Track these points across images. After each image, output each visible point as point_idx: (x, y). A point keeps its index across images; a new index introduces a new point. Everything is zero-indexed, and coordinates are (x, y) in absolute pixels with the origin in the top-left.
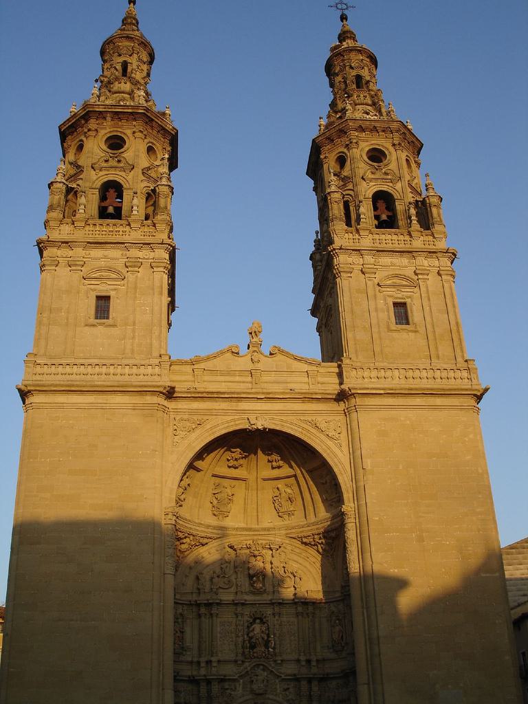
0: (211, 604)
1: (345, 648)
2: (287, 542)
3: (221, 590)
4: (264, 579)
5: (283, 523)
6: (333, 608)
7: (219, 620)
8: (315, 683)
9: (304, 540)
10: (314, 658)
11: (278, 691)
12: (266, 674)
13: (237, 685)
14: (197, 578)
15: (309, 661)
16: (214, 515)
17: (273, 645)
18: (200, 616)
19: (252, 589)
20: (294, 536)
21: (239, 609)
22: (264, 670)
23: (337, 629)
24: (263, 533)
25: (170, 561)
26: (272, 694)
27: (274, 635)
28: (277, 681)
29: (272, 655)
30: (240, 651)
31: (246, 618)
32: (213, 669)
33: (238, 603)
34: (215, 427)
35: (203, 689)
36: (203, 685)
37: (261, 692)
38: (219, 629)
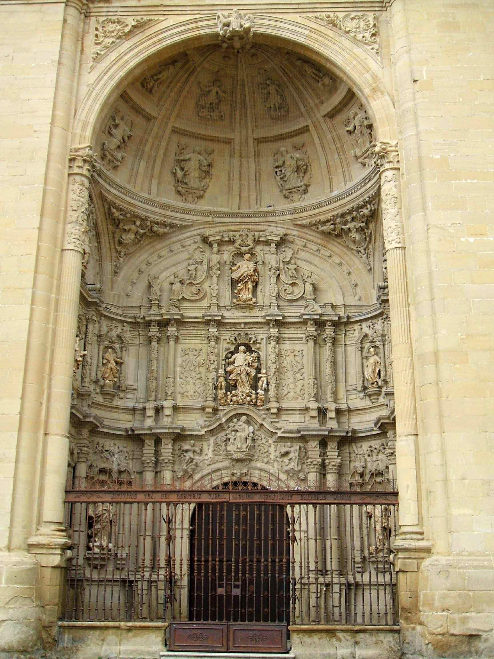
1: (384, 390)
2: (295, 233)
3: (186, 304)
4: (255, 288)
6: (366, 330)
7: (180, 347)
9: (321, 228)
10: (332, 406)
11: (272, 456)
12: (251, 429)
14: (150, 286)
16: (179, 193)
17: (265, 385)
19: (235, 301)
20: (304, 222)
21: (213, 330)
22: (248, 423)
24: (257, 220)
25: (73, 231)
27: (268, 368)
28: (271, 441)
29: (263, 402)
31: (224, 345)
32: (165, 419)
33: (211, 321)
34: (163, 31)
35: (149, 451)
36: (149, 443)
37: (240, 456)
38: (179, 360)
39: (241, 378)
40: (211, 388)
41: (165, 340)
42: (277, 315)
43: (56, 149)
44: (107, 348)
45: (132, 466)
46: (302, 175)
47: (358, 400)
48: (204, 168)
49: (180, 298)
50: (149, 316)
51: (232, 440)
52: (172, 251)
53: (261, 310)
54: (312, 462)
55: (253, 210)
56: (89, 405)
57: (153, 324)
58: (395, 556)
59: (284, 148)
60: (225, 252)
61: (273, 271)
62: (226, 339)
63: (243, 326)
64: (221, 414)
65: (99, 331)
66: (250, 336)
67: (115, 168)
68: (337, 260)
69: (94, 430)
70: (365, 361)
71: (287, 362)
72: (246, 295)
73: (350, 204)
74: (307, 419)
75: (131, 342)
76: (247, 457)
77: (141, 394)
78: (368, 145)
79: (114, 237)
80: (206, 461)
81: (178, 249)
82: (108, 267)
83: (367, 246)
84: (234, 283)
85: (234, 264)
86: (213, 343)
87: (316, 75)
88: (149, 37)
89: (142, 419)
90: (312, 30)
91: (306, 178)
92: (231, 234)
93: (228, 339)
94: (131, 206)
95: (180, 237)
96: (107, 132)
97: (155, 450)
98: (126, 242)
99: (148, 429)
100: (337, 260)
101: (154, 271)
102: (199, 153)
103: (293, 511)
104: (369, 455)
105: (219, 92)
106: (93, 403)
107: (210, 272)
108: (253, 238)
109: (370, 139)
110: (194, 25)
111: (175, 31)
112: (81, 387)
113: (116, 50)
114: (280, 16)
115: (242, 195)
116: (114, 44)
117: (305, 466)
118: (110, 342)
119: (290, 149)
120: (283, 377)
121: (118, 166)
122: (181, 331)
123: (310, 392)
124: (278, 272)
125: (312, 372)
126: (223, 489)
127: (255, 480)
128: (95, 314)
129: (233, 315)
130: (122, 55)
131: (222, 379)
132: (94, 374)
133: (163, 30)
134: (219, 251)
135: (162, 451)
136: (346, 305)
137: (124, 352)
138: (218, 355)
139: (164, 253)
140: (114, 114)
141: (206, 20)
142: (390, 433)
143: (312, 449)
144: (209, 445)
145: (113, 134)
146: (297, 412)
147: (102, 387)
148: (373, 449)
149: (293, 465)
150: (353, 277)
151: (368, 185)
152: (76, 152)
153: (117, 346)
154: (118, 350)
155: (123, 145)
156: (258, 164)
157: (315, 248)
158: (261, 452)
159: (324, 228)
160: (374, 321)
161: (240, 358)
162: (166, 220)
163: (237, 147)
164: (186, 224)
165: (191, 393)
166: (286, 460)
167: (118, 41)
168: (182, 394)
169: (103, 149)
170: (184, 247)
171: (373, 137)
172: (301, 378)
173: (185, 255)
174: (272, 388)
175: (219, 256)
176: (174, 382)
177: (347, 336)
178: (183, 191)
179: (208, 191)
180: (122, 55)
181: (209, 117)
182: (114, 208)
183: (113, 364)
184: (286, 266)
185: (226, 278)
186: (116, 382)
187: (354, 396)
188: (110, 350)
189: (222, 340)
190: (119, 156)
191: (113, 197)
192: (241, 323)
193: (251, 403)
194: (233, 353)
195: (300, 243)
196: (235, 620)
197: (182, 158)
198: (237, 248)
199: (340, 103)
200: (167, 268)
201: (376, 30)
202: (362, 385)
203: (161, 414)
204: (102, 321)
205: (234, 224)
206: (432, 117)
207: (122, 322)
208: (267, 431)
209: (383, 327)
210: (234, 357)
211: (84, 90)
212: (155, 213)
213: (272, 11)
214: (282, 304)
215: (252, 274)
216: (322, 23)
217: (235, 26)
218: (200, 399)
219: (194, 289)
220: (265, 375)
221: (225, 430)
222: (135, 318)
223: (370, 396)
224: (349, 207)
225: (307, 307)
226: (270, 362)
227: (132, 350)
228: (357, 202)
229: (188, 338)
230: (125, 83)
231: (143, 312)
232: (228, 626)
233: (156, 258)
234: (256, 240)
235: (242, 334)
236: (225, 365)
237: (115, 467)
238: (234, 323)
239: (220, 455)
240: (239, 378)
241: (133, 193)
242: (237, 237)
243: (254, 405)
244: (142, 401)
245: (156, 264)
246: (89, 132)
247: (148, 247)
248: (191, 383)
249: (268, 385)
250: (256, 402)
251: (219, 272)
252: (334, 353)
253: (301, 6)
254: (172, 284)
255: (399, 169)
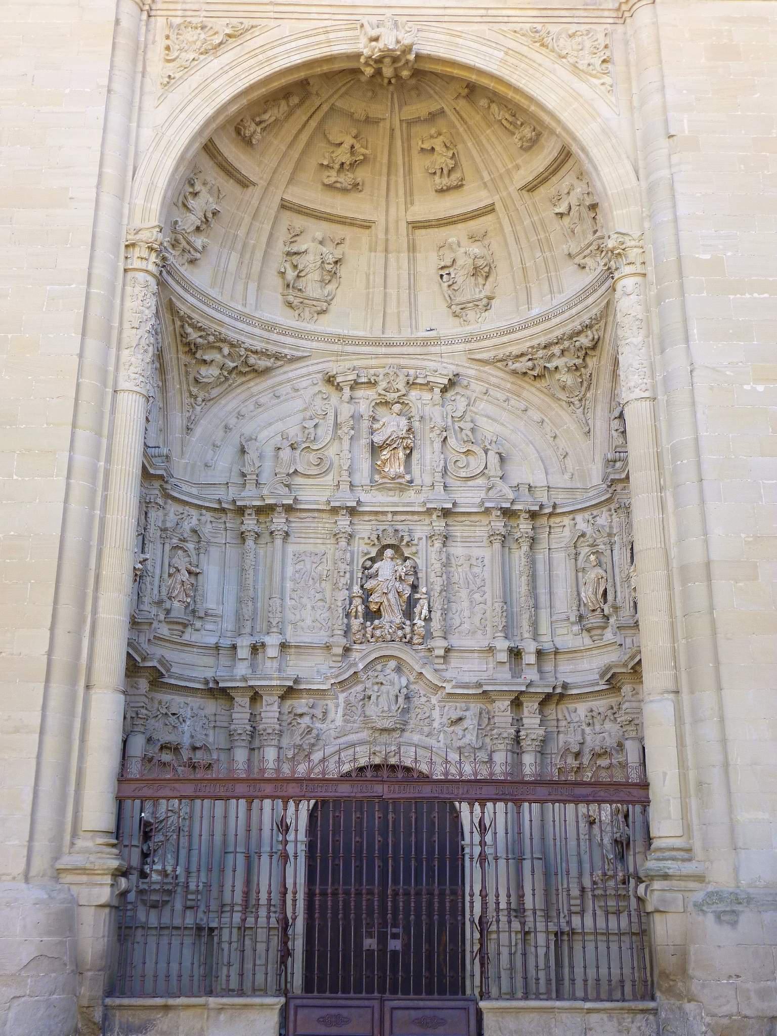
0: (271, 508)
1: (612, 620)
3: (298, 480)
4: (409, 456)
5: (459, 330)
6: (582, 526)
7: (291, 549)
8: (530, 707)
9: (512, 366)
10: (529, 648)
11: (436, 725)
13: (331, 704)
14: (243, 451)
15: (516, 654)
16: (290, 305)
17: (425, 612)
18: (242, 537)
19: (377, 477)
20: (484, 356)
21: (343, 522)
22: (398, 670)
23: (592, 574)
26: (421, 732)
28: (434, 700)
30: (341, 622)
32: (268, 664)
35: (241, 714)
36: (242, 701)
37: (388, 724)
38: (290, 570)
39: (388, 600)
40: (341, 615)
41: (266, 538)
42: (445, 501)
43: (105, 229)
44: (177, 547)
45: (215, 739)
46: (481, 280)
47: (570, 637)
48: (328, 267)
49: (291, 471)
50: (243, 499)
51: (373, 698)
52: (278, 397)
53: (419, 492)
54: (500, 734)
55: (406, 333)
56: (149, 640)
57: (248, 511)
58: (647, 887)
59: (455, 239)
60: (361, 401)
61: (438, 432)
62: (363, 538)
63: (390, 516)
64: (354, 656)
65: (164, 521)
66: (401, 534)
67: (192, 262)
68: (536, 415)
69: (157, 680)
70: (580, 574)
71: (459, 574)
72: (395, 468)
73: (559, 328)
74: (491, 666)
75: (212, 540)
76: (398, 726)
77: (229, 625)
78: (590, 237)
79: (187, 373)
80: (332, 731)
81: (287, 394)
82: (178, 420)
83: (584, 395)
84: (375, 449)
85: (374, 419)
86: (343, 543)
87: (511, 123)
88: (253, 53)
89: (228, 664)
90: (508, 51)
91: (487, 287)
92: (372, 371)
93: (366, 538)
94: (215, 323)
95: (291, 375)
96: (180, 204)
97: (251, 714)
98: (204, 380)
99: (241, 681)
100: (536, 415)
101: (248, 428)
102: (321, 243)
103: (483, 813)
104: (589, 724)
105: (357, 146)
106: (155, 637)
107: (339, 432)
108: (406, 379)
109: (593, 226)
110: (322, 37)
111: (293, 44)
112: (137, 612)
113: (198, 73)
114: (459, 27)
115: (389, 311)
116: (196, 62)
117: (488, 740)
118: (180, 540)
119: (465, 241)
120: (453, 599)
121: (196, 260)
122: (293, 525)
123: (496, 624)
124: (445, 434)
125: (498, 591)
126: (373, 776)
127: (408, 763)
128: (160, 496)
129: (374, 500)
130: (209, 81)
131: (359, 601)
132: (156, 591)
133: (275, 44)
134: (351, 398)
135: (263, 715)
136: (550, 486)
137: (202, 555)
138: (350, 564)
139: (262, 401)
140: (192, 175)
141: (341, 30)
142: (626, 689)
143: (501, 714)
144: (337, 706)
145: (190, 207)
146: (476, 655)
147: (168, 612)
148: (594, 714)
149: (471, 738)
150: (562, 443)
151: (591, 300)
152: (136, 234)
153: (190, 546)
154: (193, 552)
155: (204, 226)
156: (412, 261)
157: (501, 395)
158: (419, 716)
159: (517, 366)
160: (595, 513)
161: (386, 568)
162: (269, 347)
163: (381, 236)
164: (300, 354)
165: (308, 622)
166: (458, 729)
167: (202, 57)
168: (295, 624)
169: (174, 231)
170: (297, 390)
171: (599, 225)
172: (481, 599)
173: (298, 404)
174: (436, 616)
175: (352, 407)
176: (282, 606)
177: (552, 536)
178: (296, 302)
179: (334, 302)
180: (209, 81)
181: (338, 185)
182: (189, 325)
183: (185, 576)
184: (457, 425)
185: (364, 441)
186: (189, 603)
187: (565, 631)
188: (180, 552)
189: (357, 538)
190: (198, 241)
191: (189, 308)
192: (388, 512)
193: (404, 640)
194: (373, 560)
195: (477, 387)
196: (394, 991)
197: (295, 249)
198: (380, 395)
199: (546, 169)
200: (270, 424)
201: (608, 53)
202: (577, 613)
203: (260, 656)
204: (168, 507)
205: (377, 357)
206: (698, 195)
207: (200, 507)
208: (427, 682)
209: (611, 522)
210: (376, 566)
211: (147, 134)
212: (252, 336)
213: (446, 19)
214: (450, 481)
215: (404, 435)
216: (523, 40)
217: (389, 41)
218: (322, 633)
219: (312, 457)
220: (426, 596)
221: (362, 682)
222: (220, 502)
223: (588, 630)
224: (558, 333)
225: (490, 489)
226: (433, 575)
227: (215, 552)
228: (570, 327)
229: (303, 535)
230: (214, 126)
231: (233, 492)
232: (382, 1001)
233: (252, 407)
234: (411, 382)
235: (390, 530)
236: (361, 578)
237: (186, 741)
238: (376, 513)
239: (354, 722)
240: (385, 600)
241: (220, 303)
242: (381, 377)
243: (409, 642)
244: (229, 634)
245: (251, 418)
246: (156, 205)
247: (239, 391)
248: (309, 607)
249: (430, 612)
250: (411, 638)
251: (352, 432)
252: (532, 563)
253: (491, 12)
254: (279, 449)
255: (644, 275)
